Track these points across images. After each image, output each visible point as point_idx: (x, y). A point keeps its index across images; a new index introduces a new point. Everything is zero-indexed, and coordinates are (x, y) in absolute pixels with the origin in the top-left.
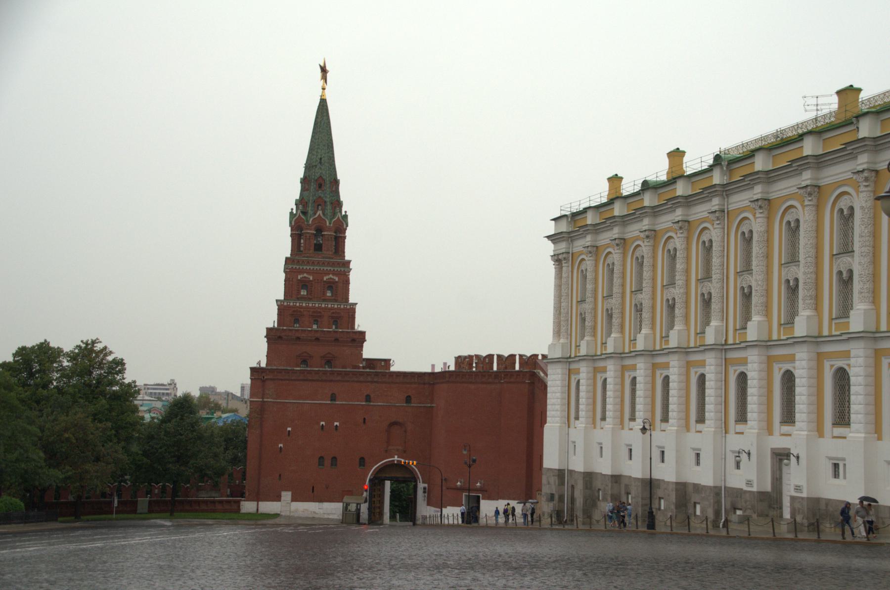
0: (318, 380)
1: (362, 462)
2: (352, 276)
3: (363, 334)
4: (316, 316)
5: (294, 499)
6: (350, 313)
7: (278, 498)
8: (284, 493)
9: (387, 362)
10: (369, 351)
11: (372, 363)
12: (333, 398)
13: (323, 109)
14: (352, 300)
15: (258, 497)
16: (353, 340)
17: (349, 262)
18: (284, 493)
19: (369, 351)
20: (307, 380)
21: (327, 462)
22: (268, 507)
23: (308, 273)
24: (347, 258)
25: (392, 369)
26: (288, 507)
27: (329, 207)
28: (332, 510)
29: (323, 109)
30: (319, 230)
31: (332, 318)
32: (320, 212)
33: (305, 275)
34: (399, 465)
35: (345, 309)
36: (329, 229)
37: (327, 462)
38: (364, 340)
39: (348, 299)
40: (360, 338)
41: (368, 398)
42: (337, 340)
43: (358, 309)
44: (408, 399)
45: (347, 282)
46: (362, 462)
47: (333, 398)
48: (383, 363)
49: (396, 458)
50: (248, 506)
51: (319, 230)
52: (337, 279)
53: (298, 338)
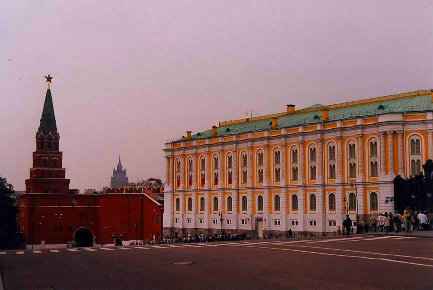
1: (71, 229)
6: (64, 172)
10: (71, 187)
16: (66, 183)
17: (62, 152)
19: (71, 187)
25: (79, 193)
36: (54, 139)
42: (59, 183)
43: (66, 170)
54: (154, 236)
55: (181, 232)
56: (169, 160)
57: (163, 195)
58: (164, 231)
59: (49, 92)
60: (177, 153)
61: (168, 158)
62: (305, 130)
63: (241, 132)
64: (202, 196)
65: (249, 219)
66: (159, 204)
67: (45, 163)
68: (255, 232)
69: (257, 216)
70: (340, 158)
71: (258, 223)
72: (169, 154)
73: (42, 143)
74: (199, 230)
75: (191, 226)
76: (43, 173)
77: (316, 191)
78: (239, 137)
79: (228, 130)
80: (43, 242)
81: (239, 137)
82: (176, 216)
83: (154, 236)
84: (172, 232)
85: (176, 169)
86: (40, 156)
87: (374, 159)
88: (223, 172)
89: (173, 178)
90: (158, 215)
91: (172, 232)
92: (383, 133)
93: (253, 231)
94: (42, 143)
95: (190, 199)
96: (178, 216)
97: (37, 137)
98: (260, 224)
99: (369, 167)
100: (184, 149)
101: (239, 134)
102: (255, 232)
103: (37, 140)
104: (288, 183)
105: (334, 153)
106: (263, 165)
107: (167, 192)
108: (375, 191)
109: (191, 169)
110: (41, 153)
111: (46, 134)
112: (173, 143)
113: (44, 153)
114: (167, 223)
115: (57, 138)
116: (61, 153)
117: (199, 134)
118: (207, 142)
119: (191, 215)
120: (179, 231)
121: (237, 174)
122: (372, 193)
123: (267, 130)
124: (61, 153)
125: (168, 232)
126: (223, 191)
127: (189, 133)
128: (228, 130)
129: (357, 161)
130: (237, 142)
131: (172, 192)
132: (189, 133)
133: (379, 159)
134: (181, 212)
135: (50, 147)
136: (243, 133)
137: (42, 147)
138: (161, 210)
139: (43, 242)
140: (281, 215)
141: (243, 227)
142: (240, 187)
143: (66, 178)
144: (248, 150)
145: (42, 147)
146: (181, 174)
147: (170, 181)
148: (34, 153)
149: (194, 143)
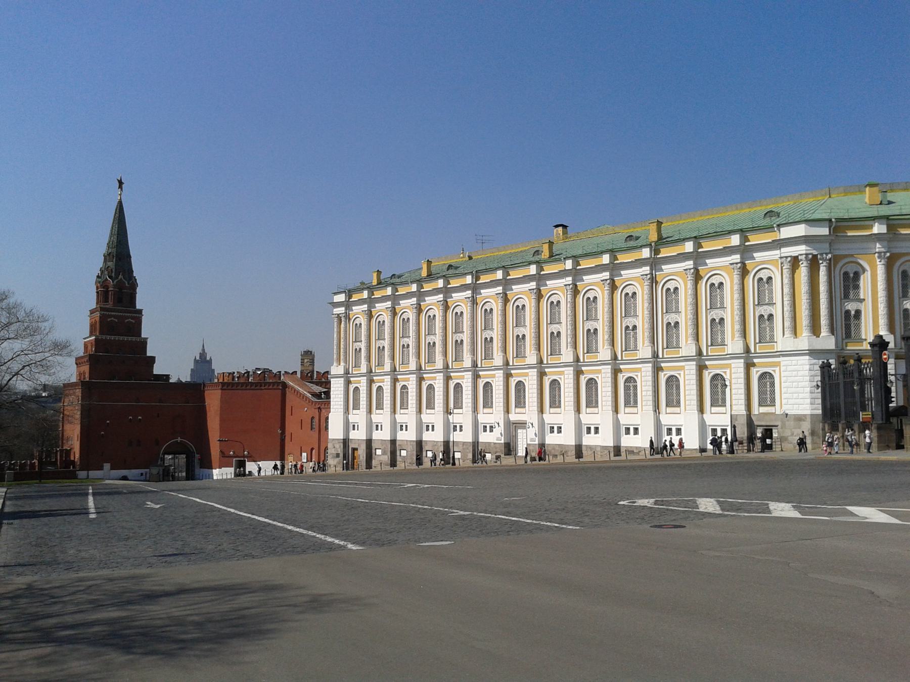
2: (144, 319)
3: (153, 359)
5: (112, 469)
7: (101, 468)
9: (167, 377)
10: (157, 370)
14: (144, 335)
19: (157, 370)
24: (138, 307)
39: (140, 335)
49: (179, 439)
54: (304, 455)
57: (327, 384)
58: (330, 446)
59: (120, 205)
80: (107, 466)
83: (304, 455)
92: (789, 259)
96: (358, 417)
114: (335, 431)
115: (133, 285)
116: (140, 312)
124: (140, 312)
125: (337, 446)
133: (779, 310)
139: (107, 466)
143: (148, 354)
147: (342, 357)
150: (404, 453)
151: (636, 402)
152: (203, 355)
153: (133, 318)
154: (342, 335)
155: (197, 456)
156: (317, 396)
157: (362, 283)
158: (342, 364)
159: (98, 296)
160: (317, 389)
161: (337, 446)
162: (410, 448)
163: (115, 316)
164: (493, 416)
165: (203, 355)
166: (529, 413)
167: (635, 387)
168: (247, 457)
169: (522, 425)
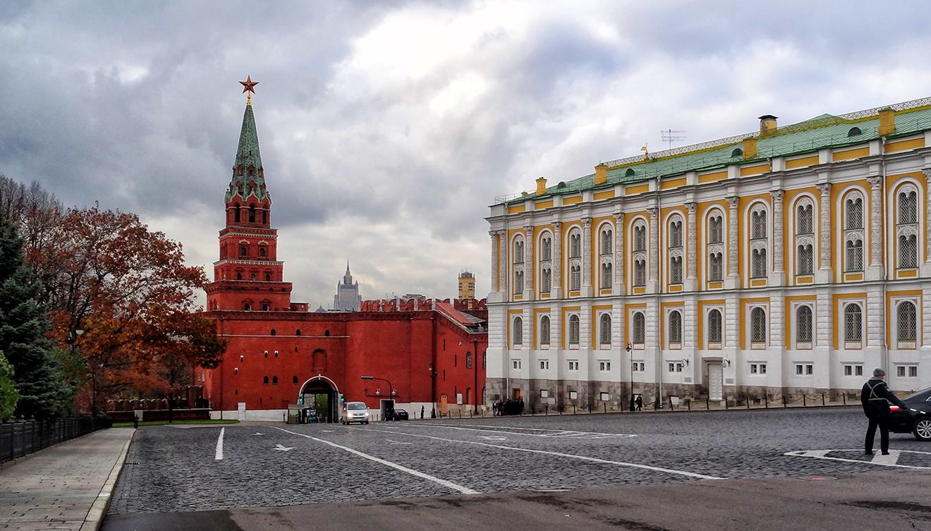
0: (261, 320)
1: (295, 380)
4: (254, 271)
5: (247, 409)
6: (279, 269)
7: (236, 408)
8: (239, 404)
10: (296, 297)
11: (294, 306)
12: (273, 332)
13: (249, 113)
15: (221, 407)
16: (284, 290)
18: (239, 404)
19: (296, 297)
20: (254, 320)
21: (271, 380)
22: (229, 415)
23: (246, 239)
26: (242, 414)
27: (259, 188)
28: (274, 415)
29: (249, 113)
30: (252, 206)
31: (266, 272)
32: (253, 192)
33: (244, 240)
34: (323, 382)
35: (275, 266)
37: (271, 380)
38: (290, 289)
40: (287, 288)
41: (298, 333)
44: (327, 333)
45: (275, 246)
46: (295, 380)
47: (273, 332)
48: (303, 307)
50: (215, 415)
51: (252, 206)
52: (267, 243)
53: (243, 288)
54: (460, 396)
55: (526, 387)
56: (498, 240)
58: (488, 386)
60: (516, 225)
61: (496, 235)
62: (741, 175)
63: (670, 172)
64: (516, 316)
65: (688, 362)
66: (470, 331)
67: (244, 251)
68: (702, 391)
69: (707, 353)
70: (826, 230)
71: (708, 370)
72: (501, 226)
73: (238, 211)
74: (566, 384)
75: (551, 374)
76: (239, 272)
77: (611, 307)
78: (662, 185)
79: (630, 173)
80: (242, 406)
81: (662, 185)
82: (514, 354)
83: (460, 396)
84: (505, 388)
85: (512, 258)
86: (234, 237)
87: (716, 249)
88: (592, 263)
89: (507, 277)
90: (469, 353)
91: (505, 388)
93: (698, 387)
94: (238, 211)
95: (546, 320)
96: (521, 352)
97: (227, 200)
98: (714, 373)
99: (794, 258)
100: (533, 215)
101: (663, 177)
102: (702, 391)
103: (227, 206)
104: (563, 293)
105: (721, 230)
106: (681, 246)
107: (496, 305)
108: (640, 310)
109: (547, 258)
110: (235, 230)
111: (245, 193)
112: (510, 203)
113: (242, 231)
114: (494, 367)
117: (562, 185)
118: (586, 198)
119: (549, 353)
120: (522, 386)
121: (659, 264)
122: (673, 312)
123: (733, 164)
126: (561, 305)
127: (541, 181)
128: (630, 173)
129: (649, 257)
130: (658, 196)
131: (506, 304)
132: (541, 181)
134: (526, 346)
135: (252, 219)
136: (673, 175)
137: (237, 219)
138: (480, 340)
139: (242, 406)
140: (772, 353)
141: (674, 378)
142: (664, 291)
144: (582, 224)
145: (237, 219)
146: (525, 268)
147: (502, 282)
148: (222, 233)
149: (557, 202)
150: (574, 396)
151: (859, 335)
152: (348, 278)
153: (267, 239)
154: (502, 256)
155: (340, 395)
156: (475, 327)
157: (524, 194)
158: (502, 290)
159: (228, 215)
160: (473, 320)
161: (496, 386)
162: (580, 390)
163: (247, 238)
164: (686, 351)
165: (348, 278)
166: (727, 350)
167: (859, 317)
168: (395, 397)
169: (718, 362)
